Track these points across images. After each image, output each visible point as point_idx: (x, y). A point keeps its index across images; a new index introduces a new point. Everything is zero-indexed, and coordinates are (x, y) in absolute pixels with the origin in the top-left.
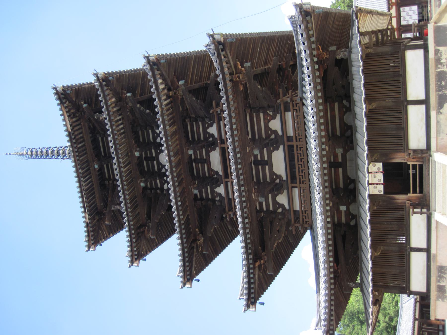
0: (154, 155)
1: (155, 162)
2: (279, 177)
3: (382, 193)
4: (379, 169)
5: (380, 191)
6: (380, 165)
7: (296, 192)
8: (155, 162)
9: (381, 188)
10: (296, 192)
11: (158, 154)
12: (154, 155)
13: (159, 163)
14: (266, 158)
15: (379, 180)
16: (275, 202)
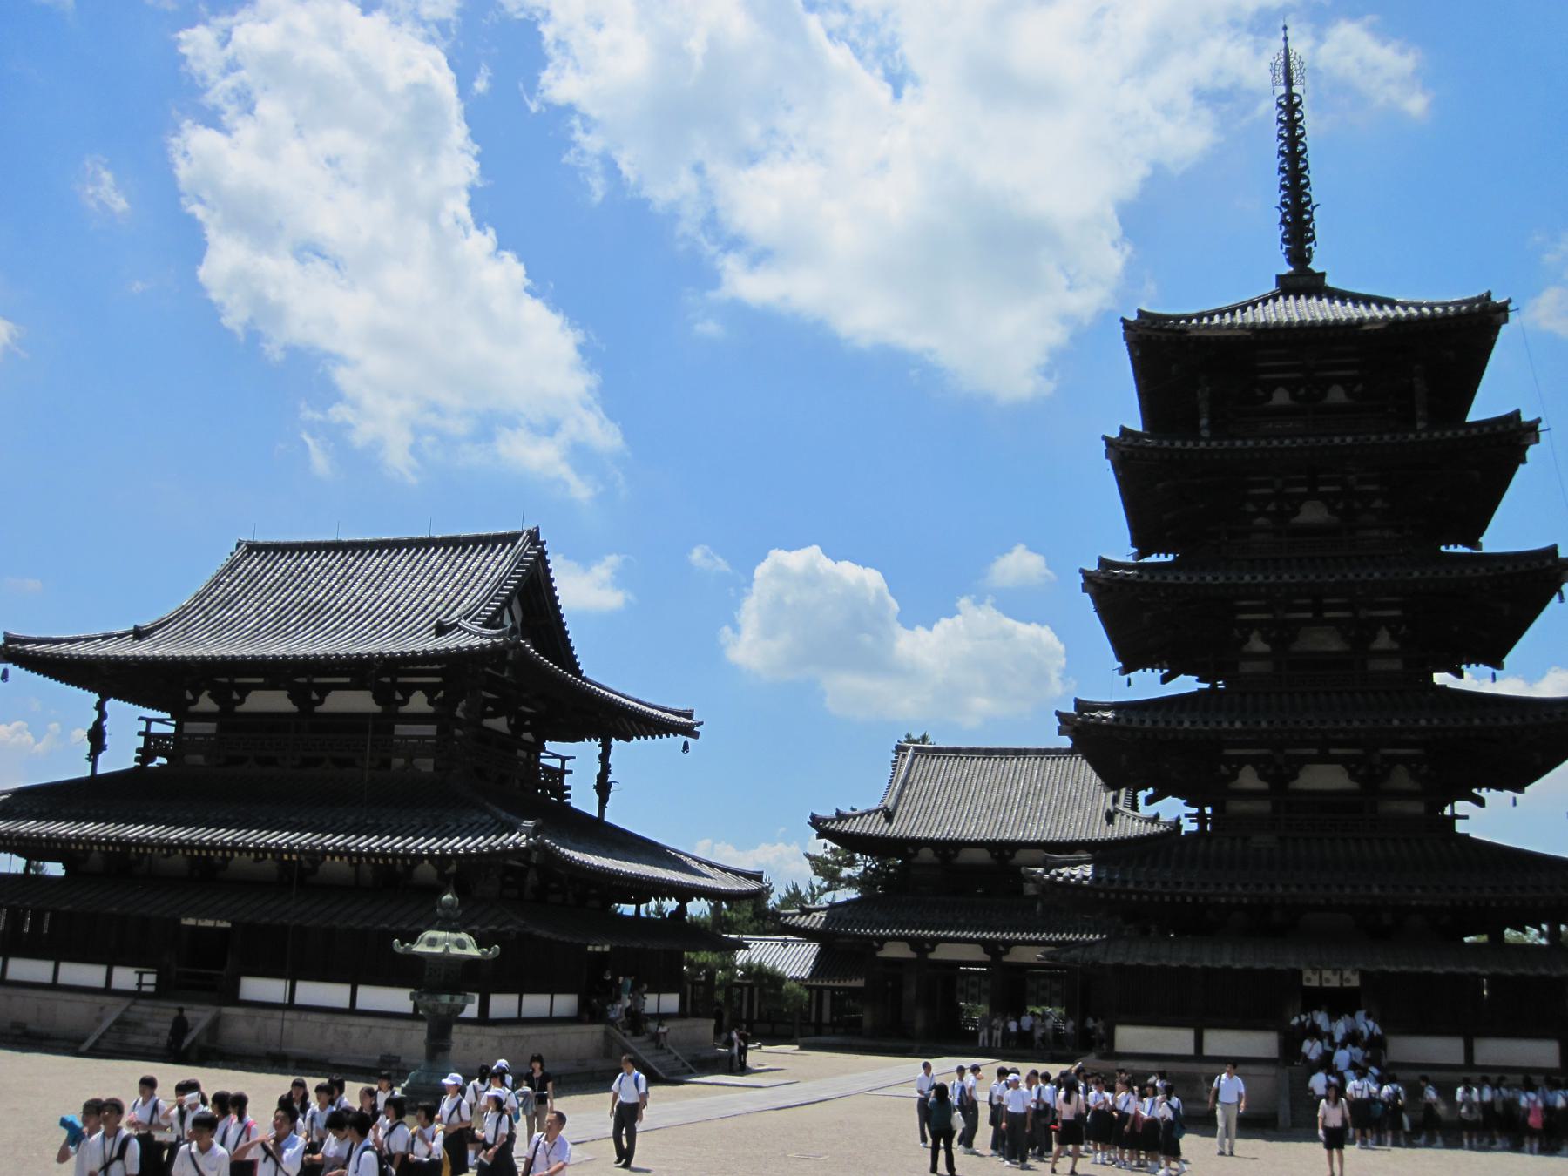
0: (1322, 489)
1: (1304, 490)
2: (1295, 777)
3: (1305, 984)
4: (1348, 980)
5: (1309, 980)
6: (1355, 981)
7: (1263, 806)
8: (1304, 490)
9: (1315, 983)
10: (1263, 806)
11: (1324, 497)
12: (1322, 489)
13: (1303, 498)
14: (1333, 751)
15: (1328, 980)
16: (1242, 761)
